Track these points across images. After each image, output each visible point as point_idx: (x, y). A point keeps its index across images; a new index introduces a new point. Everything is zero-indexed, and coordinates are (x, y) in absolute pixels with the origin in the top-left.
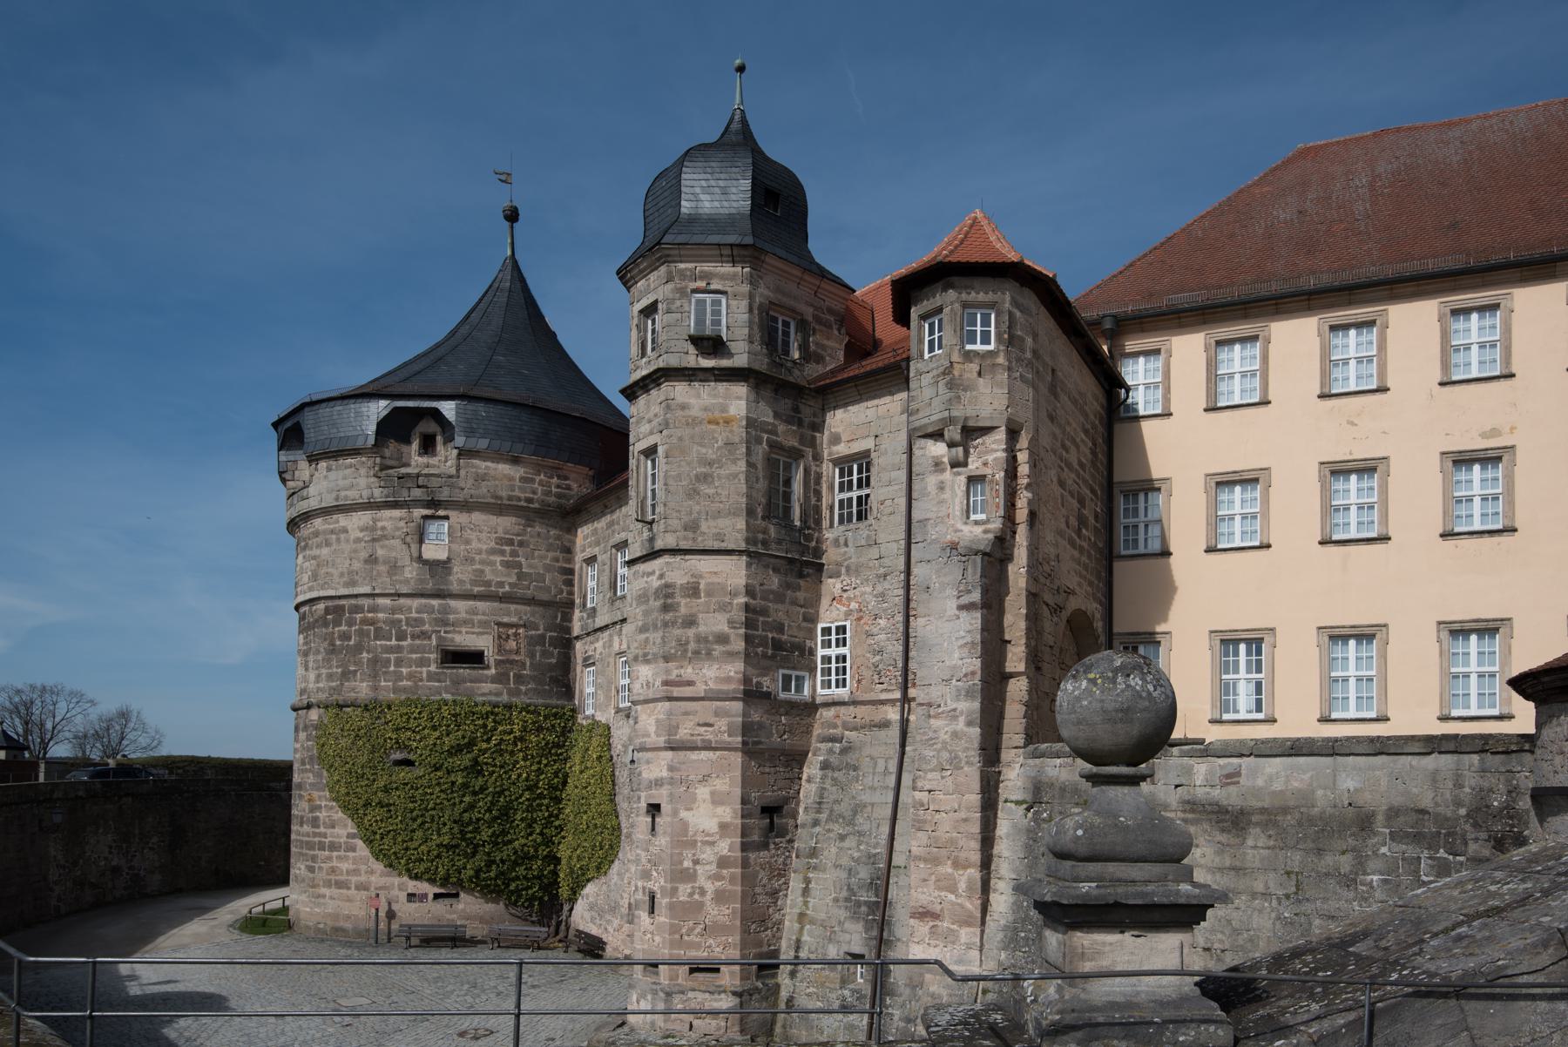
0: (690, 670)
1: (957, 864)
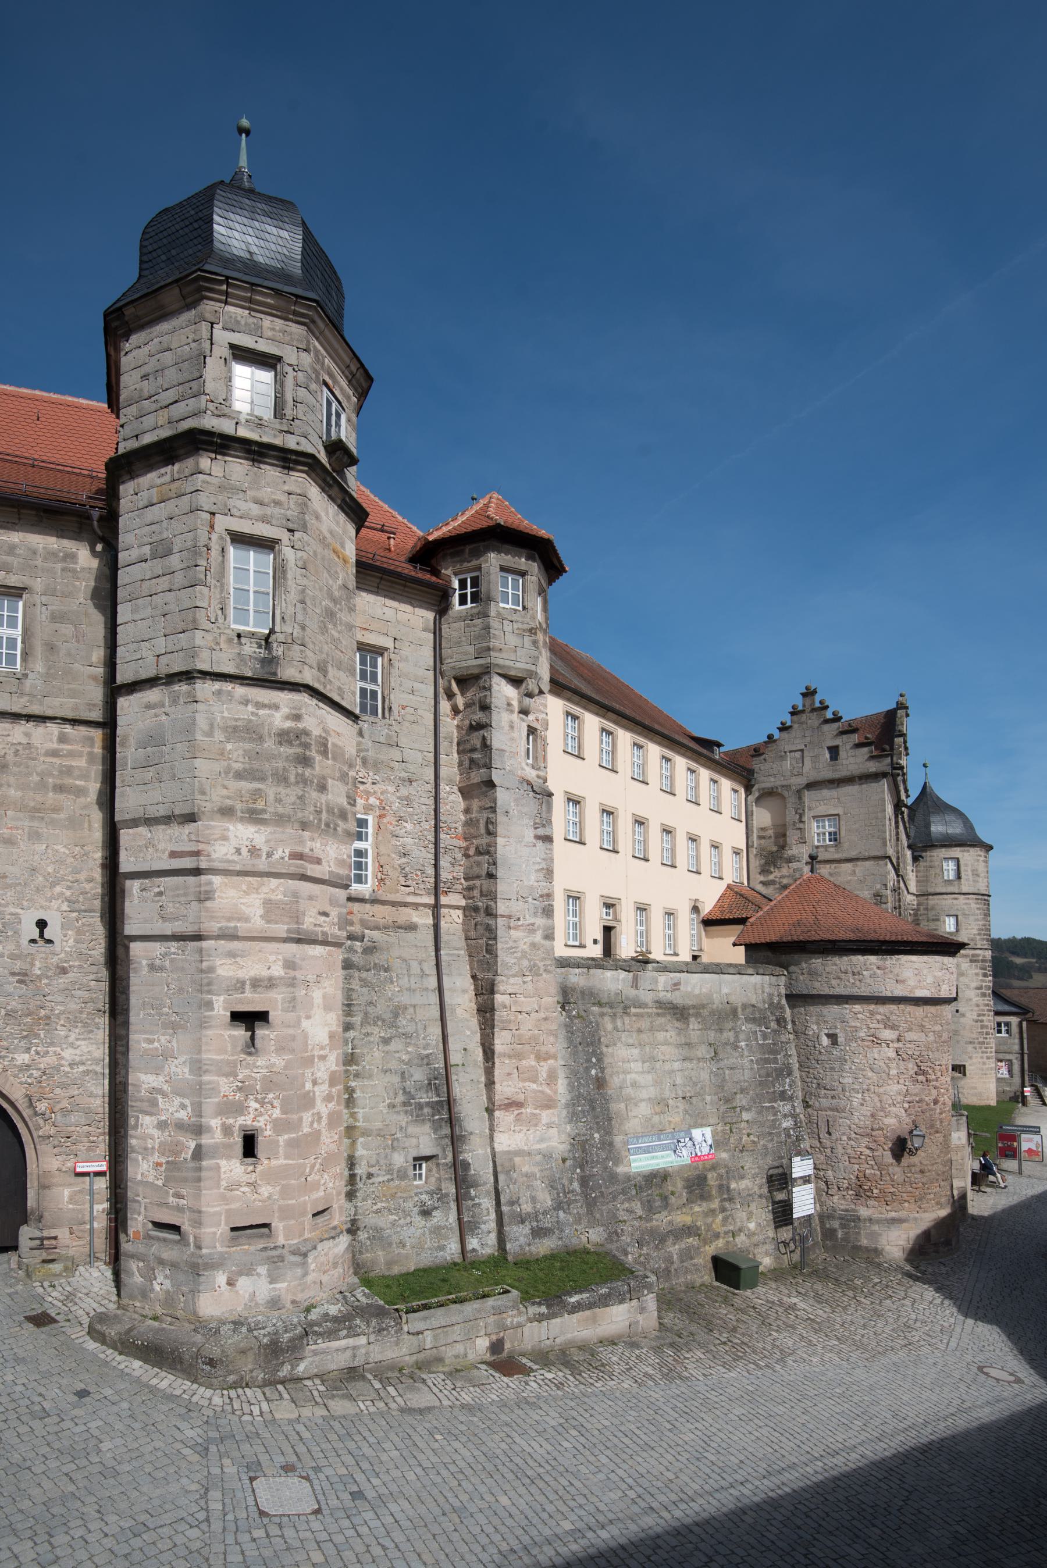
0: (318, 845)
1: (539, 1058)
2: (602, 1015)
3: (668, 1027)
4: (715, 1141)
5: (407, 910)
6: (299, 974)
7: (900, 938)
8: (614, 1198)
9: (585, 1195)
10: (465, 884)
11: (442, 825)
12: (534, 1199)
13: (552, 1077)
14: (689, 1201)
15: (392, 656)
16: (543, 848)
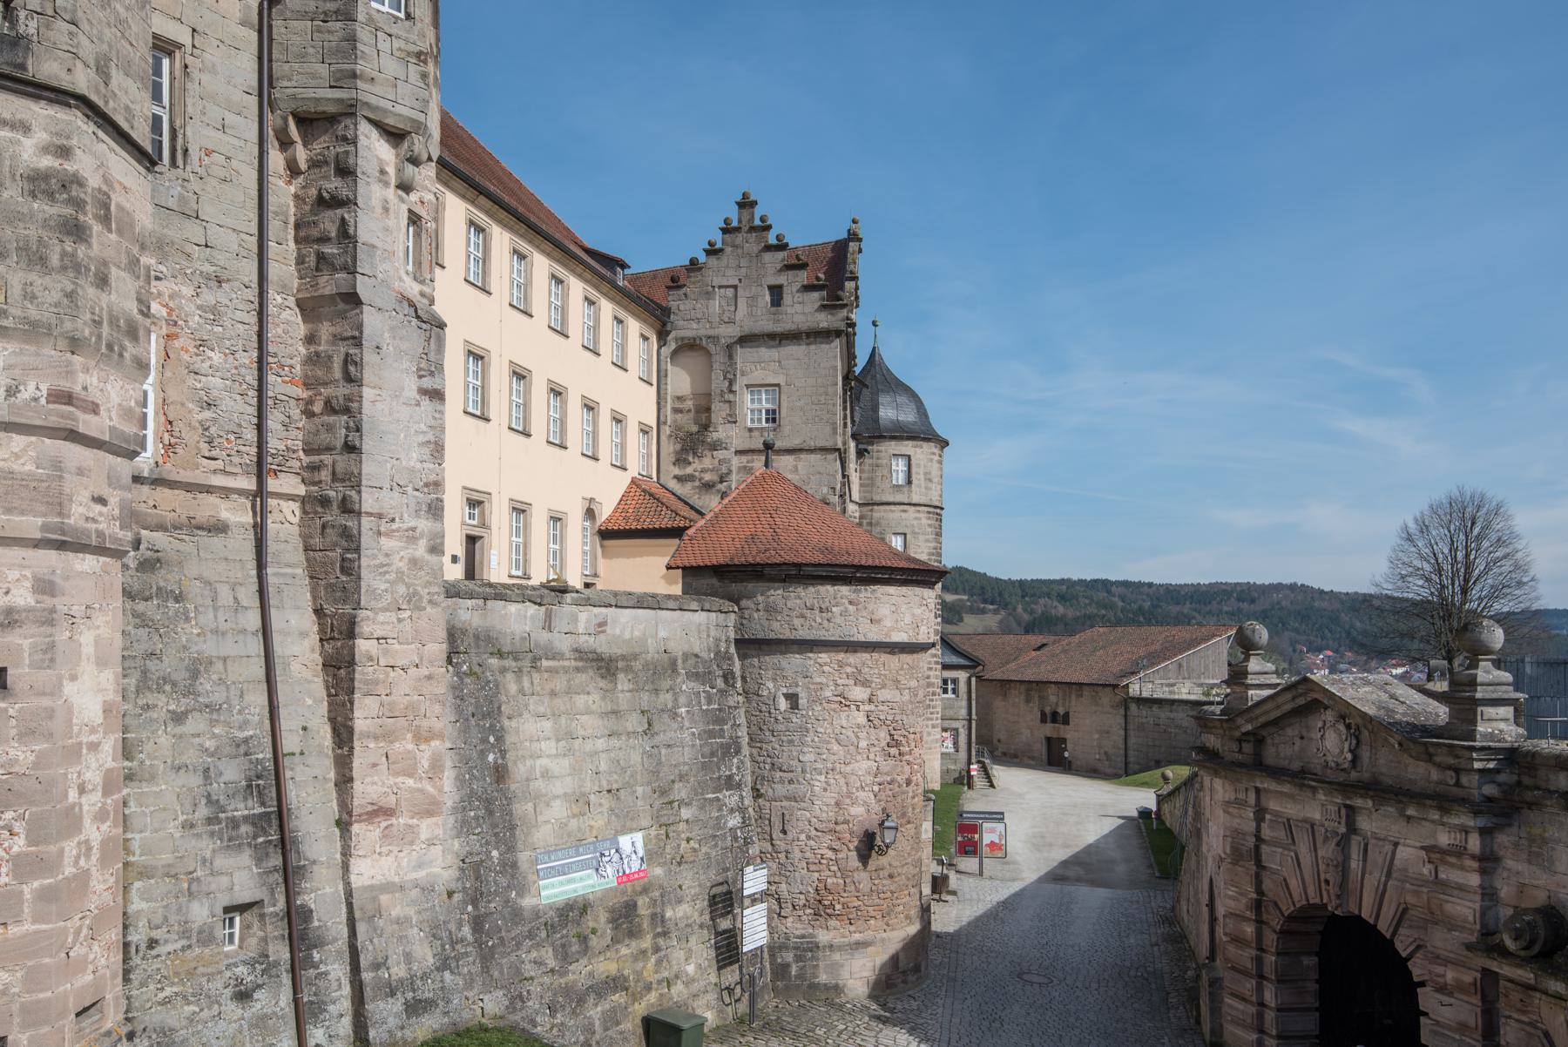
0: (95, 380)
1: (420, 738)
2: (503, 670)
3: (591, 688)
4: (647, 851)
5: (212, 499)
6: (60, 603)
7: (877, 563)
8: (518, 945)
9: (479, 943)
10: (306, 460)
11: (270, 360)
12: (408, 958)
13: (436, 766)
14: (615, 940)
15: (189, 60)
16: (430, 409)
